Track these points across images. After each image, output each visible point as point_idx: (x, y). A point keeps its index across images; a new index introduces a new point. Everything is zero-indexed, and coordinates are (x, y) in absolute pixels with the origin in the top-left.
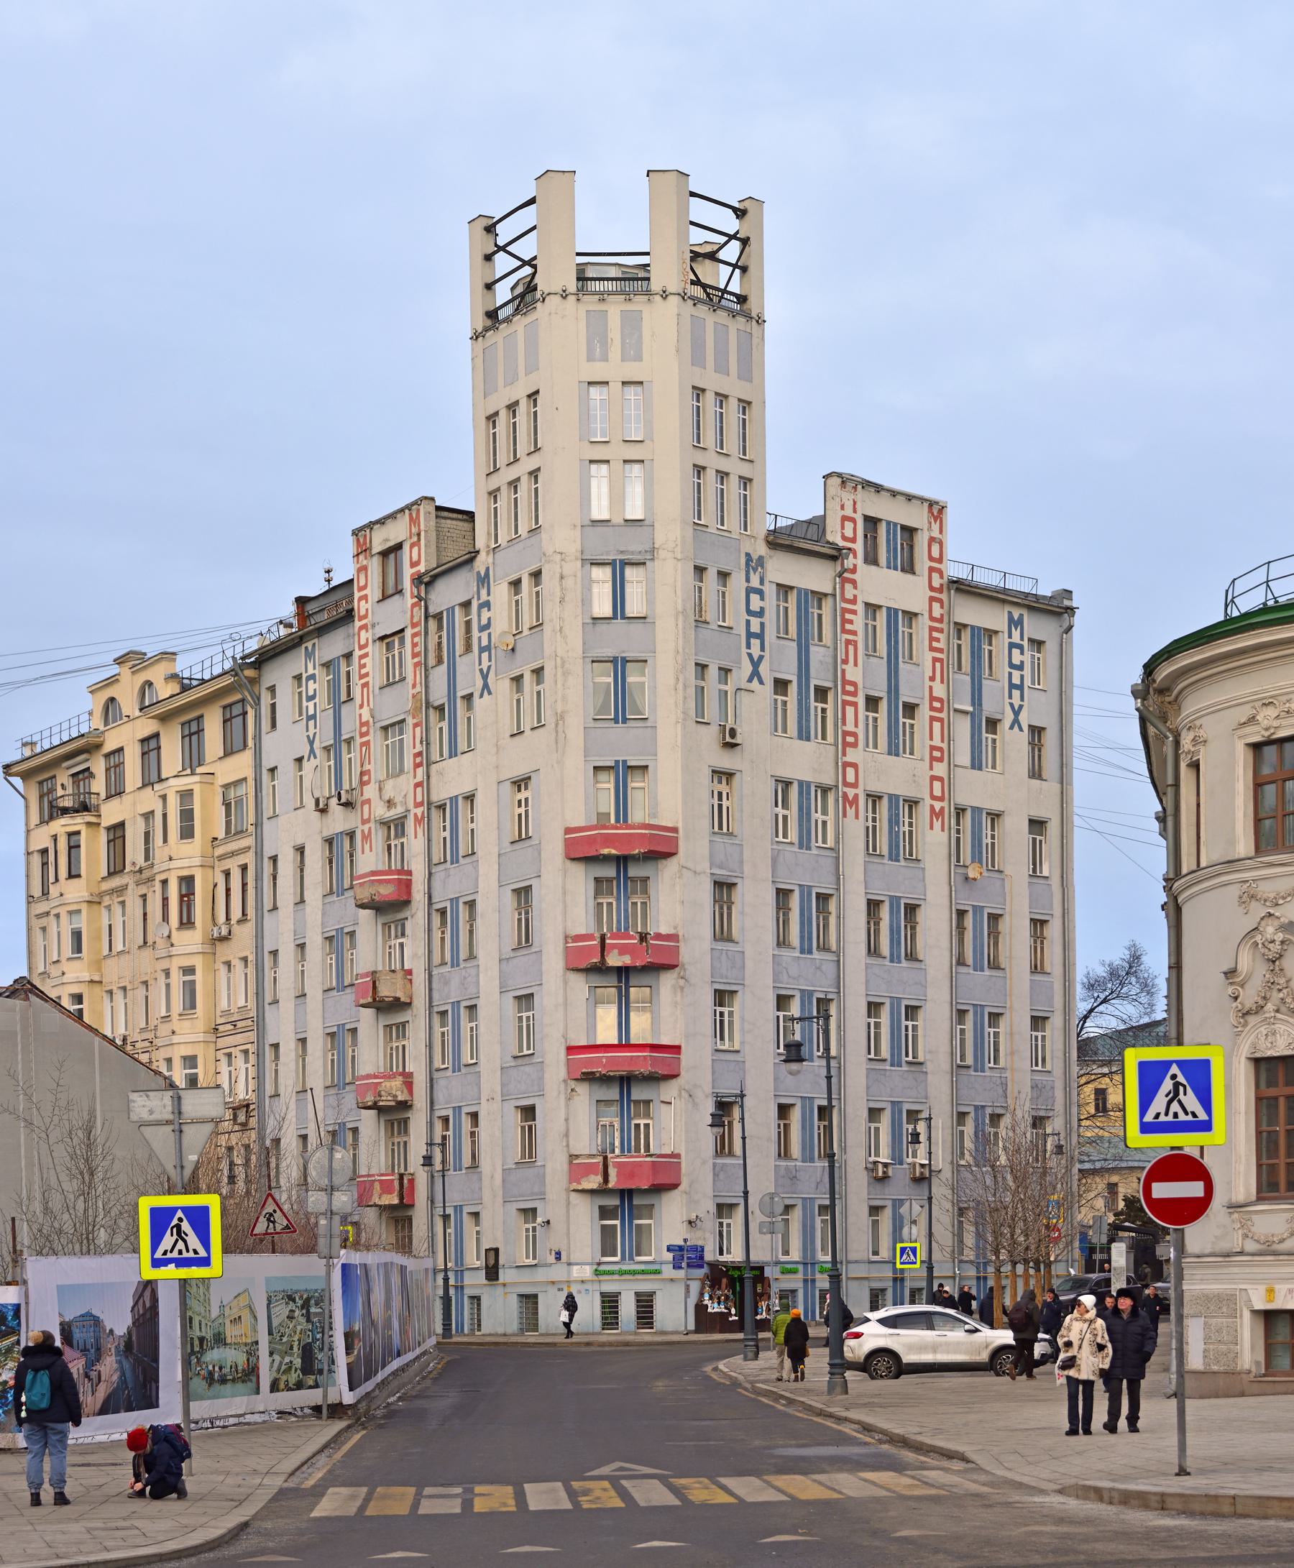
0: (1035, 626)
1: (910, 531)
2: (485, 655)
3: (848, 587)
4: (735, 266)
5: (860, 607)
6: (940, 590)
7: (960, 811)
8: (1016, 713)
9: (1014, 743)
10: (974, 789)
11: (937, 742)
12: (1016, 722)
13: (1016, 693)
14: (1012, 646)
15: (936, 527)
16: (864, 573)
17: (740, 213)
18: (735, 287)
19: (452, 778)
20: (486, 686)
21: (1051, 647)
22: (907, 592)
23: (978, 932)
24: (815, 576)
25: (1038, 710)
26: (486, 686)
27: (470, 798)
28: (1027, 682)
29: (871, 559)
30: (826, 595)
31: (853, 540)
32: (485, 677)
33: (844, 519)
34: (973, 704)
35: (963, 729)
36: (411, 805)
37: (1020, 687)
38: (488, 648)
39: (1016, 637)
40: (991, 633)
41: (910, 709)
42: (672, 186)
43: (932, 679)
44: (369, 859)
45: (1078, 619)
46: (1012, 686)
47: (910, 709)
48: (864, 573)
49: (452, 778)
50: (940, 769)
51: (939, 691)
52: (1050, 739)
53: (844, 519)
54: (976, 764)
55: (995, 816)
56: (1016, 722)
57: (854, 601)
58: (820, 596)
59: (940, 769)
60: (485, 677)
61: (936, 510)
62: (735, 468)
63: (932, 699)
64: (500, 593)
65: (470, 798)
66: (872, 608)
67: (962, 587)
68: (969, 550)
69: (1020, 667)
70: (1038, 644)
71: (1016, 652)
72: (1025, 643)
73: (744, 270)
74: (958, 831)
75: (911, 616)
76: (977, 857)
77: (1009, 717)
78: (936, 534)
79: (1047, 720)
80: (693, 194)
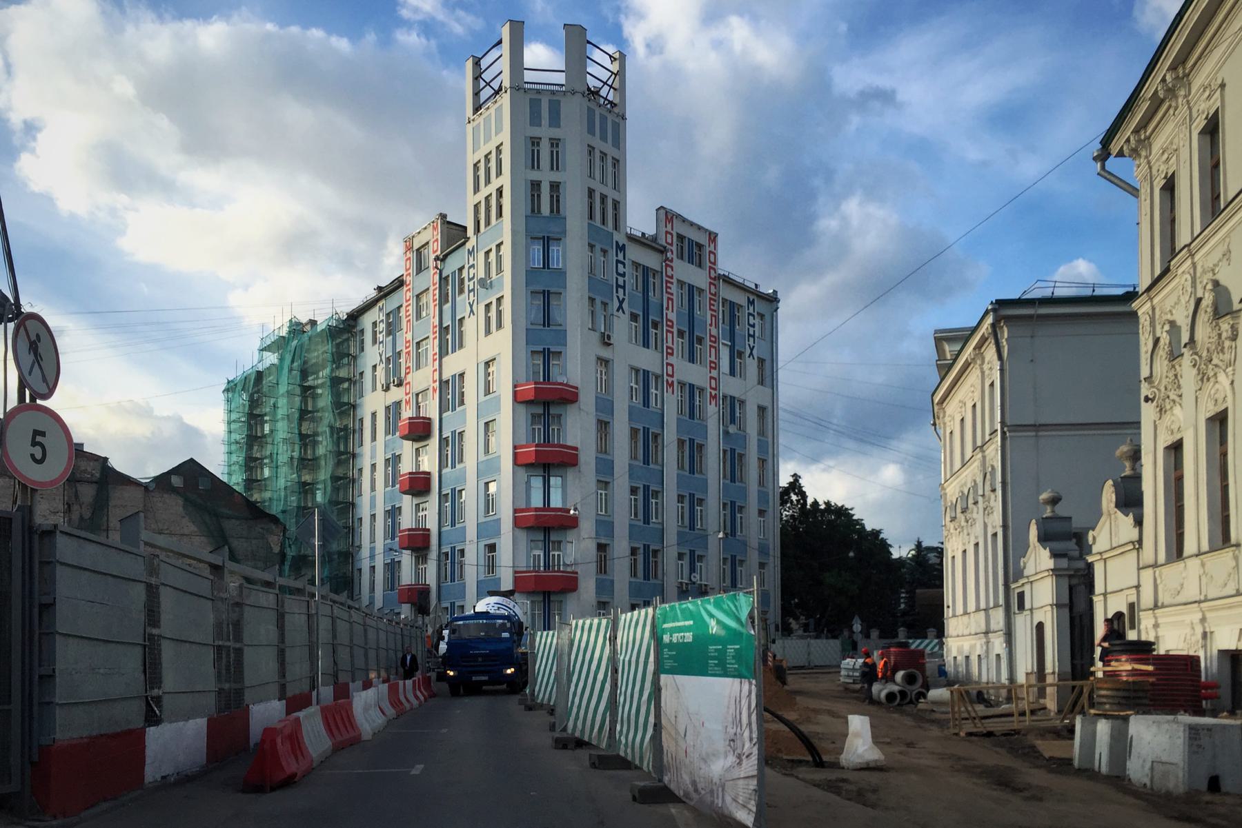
0: (760, 306)
1: (700, 246)
3: (669, 269)
5: (674, 281)
6: (715, 279)
8: (752, 349)
9: (751, 366)
10: (731, 386)
11: (713, 358)
12: (751, 354)
16: (677, 263)
19: (453, 364)
20: (472, 311)
21: (767, 318)
22: (698, 278)
23: (734, 461)
24: (651, 260)
26: (472, 311)
27: (462, 375)
31: (671, 244)
32: (471, 306)
33: (667, 232)
35: (725, 354)
37: (753, 336)
39: (751, 310)
44: (407, 413)
45: (780, 305)
47: (700, 340)
48: (677, 263)
49: (453, 364)
50: (714, 373)
51: (714, 332)
53: (667, 232)
54: (732, 372)
55: (742, 402)
56: (751, 354)
57: (672, 277)
58: (655, 272)
59: (714, 373)
60: (471, 306)
61: (713, 237)
64: (481, 256)
65: (462, 375)
66: (681, 283)
69: (753, 326)
75: (701, 291)
76: (733, 421)
77: (748, 351)
78: (712, 248)
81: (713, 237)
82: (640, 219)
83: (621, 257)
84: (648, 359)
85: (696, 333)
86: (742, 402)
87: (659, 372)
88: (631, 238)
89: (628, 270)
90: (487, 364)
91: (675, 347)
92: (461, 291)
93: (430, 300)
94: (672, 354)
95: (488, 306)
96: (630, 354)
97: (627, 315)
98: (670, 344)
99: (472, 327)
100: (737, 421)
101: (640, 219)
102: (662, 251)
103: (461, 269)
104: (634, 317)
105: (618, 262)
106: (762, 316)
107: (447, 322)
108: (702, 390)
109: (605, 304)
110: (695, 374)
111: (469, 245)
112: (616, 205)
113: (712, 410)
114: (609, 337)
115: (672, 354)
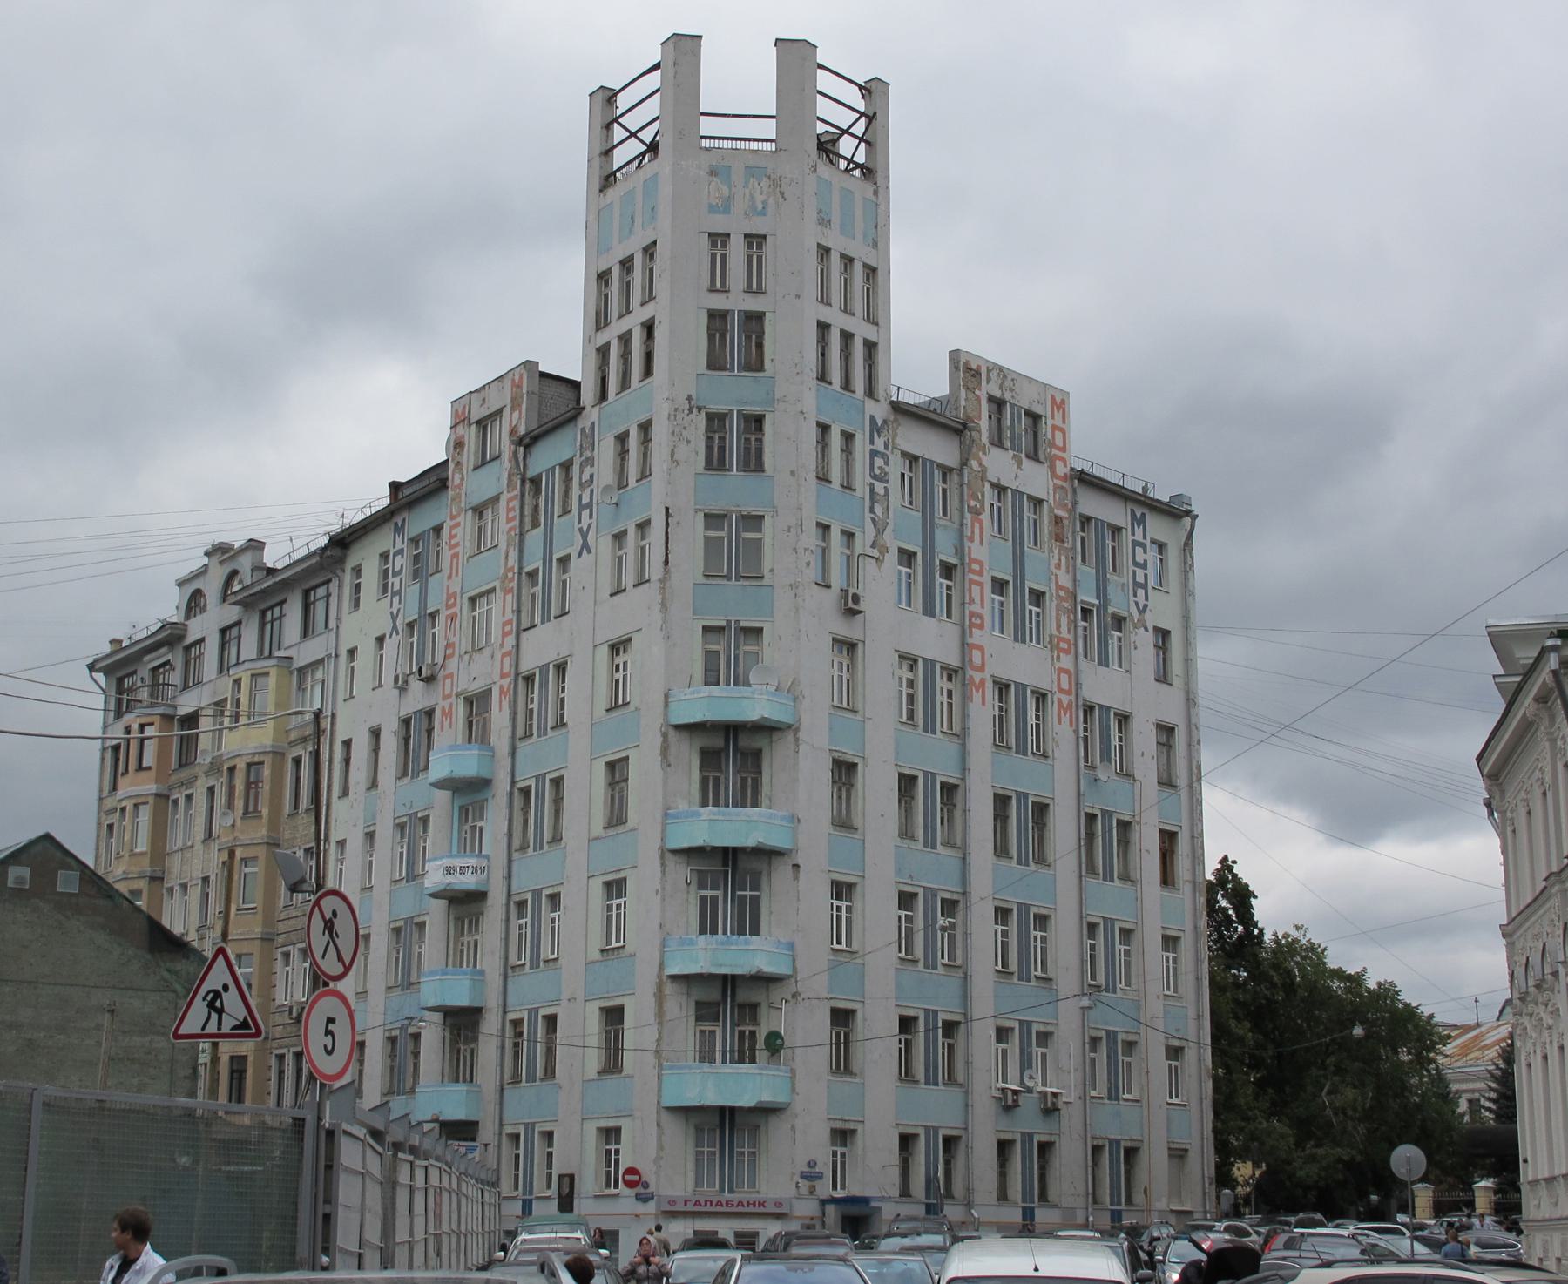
0: (1157, 527)
2: (586, 513)
4: (861, 139)
7: (1089, 709)
10: (1103, 686)
13: (1141, 592)
14: (1135, 544)
15: (1058, 416)
17: (866, 90)
18: (860, 158)
20: (585, 545)
22: (1035, 480)
25: (1163, 611)
26: (585, 545)
27: (561, 668)
28: (1151, 583)
29: (998, 443)
30: (951, 470)
32: (584, 536)
34: (1098, 598)
36: (496, 677)
37: (1144, 586)
38: (589, 506)
39: (1139, 536)
40: (1116, 530)
41: (1037, 597)
42: (796, 58)
43: (1058, 566)
46: (1137, 584)
47: (1037, 597)
52: (1176, 641)
60: (584, 536)
62: (862, 331)
63: (1059, 587)
67: (1086, 480)
68: (1090, 442)
70: (1161, 547)
71: (1139, 550)
72: (1148, 542)
73: (868, 143)
74: (1085, 730)
76: (1106, 756)
78: (1058, 422)
79: (1171, 622)
80: (821, 67)
81: (1060, 404)
82: (915, 372)
83: (879, 444)
84: (935, 640)
85: (1028, 584)
86: (1124, 719)
87: (954, 660)
88: (898, 408)
89: (896, 466)
90: (617, 647)
91: (986, 612)
92: (566, 511)
93: (501, 525)
94: (981, 627)
95: (619, 537)
96: (898, 626)
97: (892, 558)
98: (976, 608)
99: (587, 577)
100: (1115, 756)
101: (915, 372)
102: (959, 430)
103: (566, 466)
104: (907, 557)
105: (874, 454)
106: (1161, 547)
107: (534, 562)
108: (1041, 697)
109: (849, 536)
110: (1027, 664)
111: (583, 422)
112: (870, 346)
113: (1062, 733)
114: (856, 599)
115: (981, 627)
